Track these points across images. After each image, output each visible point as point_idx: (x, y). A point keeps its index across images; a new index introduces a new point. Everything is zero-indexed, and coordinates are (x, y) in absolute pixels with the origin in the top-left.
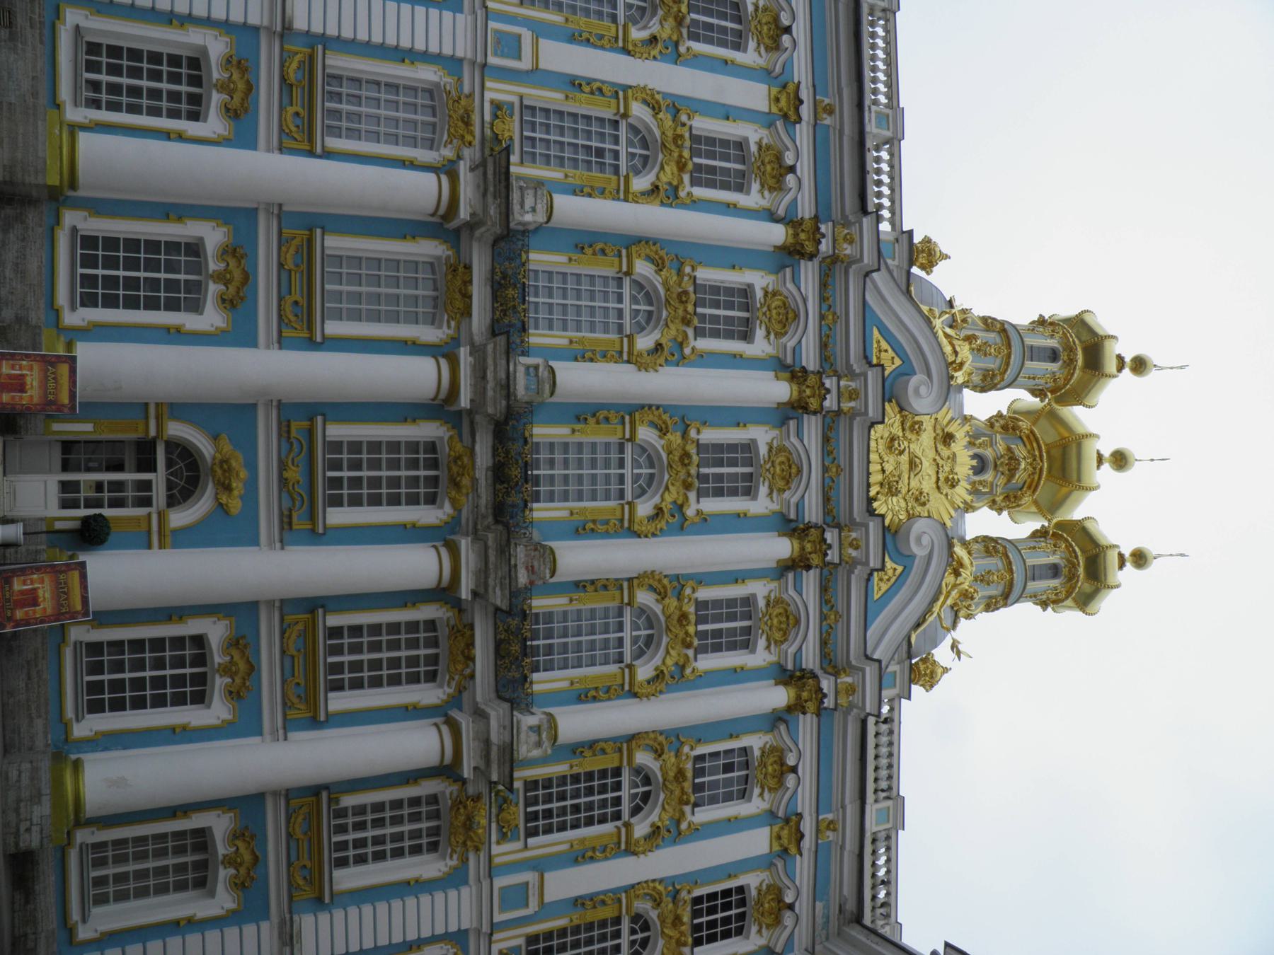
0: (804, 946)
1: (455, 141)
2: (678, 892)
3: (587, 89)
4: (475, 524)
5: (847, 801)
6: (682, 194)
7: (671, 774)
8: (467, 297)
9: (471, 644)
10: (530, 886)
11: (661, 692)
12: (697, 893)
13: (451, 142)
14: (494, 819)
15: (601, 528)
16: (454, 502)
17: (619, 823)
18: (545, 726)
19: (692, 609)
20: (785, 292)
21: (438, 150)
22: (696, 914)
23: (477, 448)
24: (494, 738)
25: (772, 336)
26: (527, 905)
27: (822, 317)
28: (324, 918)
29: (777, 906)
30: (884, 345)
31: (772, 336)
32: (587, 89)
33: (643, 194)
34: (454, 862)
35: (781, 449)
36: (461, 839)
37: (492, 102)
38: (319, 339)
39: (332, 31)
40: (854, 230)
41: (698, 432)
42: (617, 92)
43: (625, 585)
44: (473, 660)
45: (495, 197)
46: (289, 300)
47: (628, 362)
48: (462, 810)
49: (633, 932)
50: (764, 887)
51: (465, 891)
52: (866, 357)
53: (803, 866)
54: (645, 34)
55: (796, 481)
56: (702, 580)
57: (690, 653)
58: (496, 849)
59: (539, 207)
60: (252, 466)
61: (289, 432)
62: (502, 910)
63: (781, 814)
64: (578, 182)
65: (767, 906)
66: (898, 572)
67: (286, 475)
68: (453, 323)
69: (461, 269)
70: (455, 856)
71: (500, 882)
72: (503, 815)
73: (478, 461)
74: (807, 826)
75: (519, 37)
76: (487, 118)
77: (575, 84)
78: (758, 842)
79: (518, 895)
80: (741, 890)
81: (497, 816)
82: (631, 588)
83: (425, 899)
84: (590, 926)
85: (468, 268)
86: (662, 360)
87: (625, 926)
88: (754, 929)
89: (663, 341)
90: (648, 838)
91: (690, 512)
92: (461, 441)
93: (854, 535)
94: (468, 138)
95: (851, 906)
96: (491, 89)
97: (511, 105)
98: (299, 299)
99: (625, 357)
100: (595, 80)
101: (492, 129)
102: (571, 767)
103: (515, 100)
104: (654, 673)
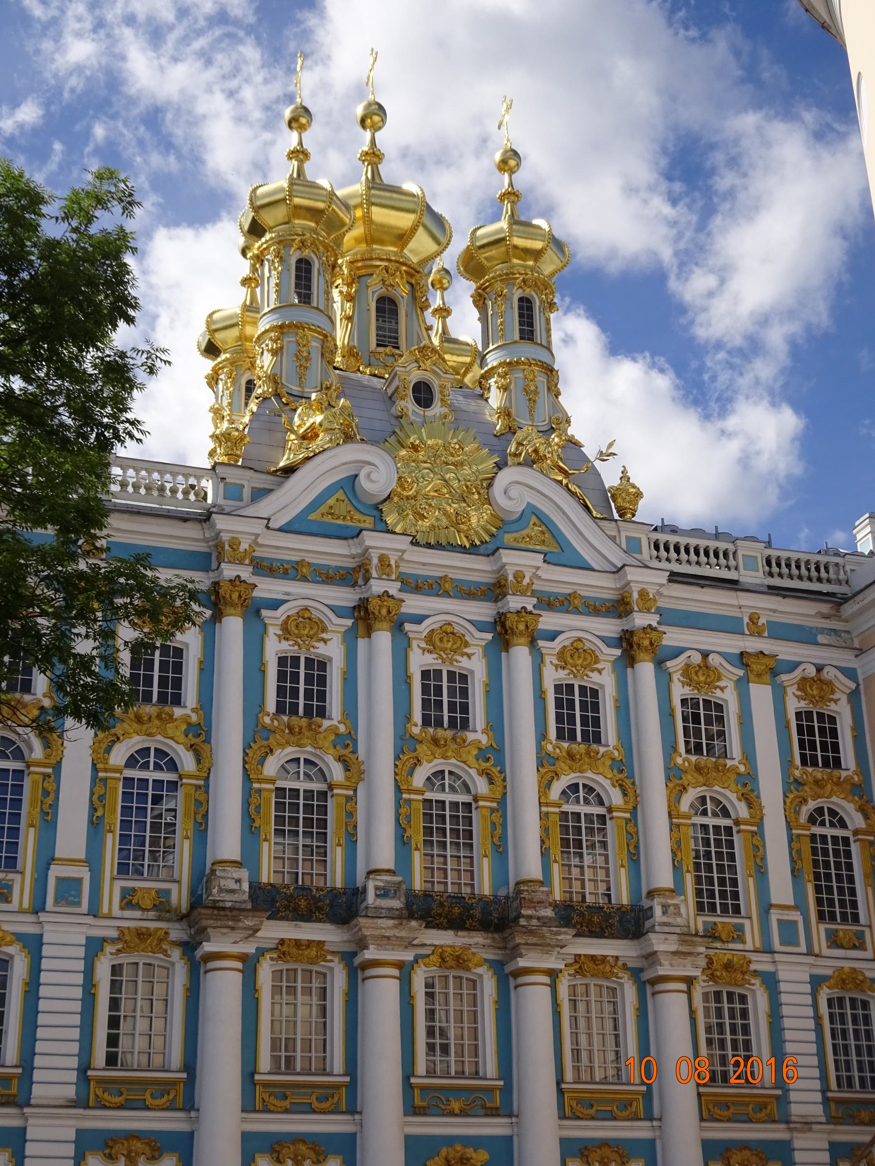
0: (853, 658)
1: (164, 947)
2: (796, 780)
3: (99, 813)
4: (499, 948)
5: (735, 603)
6: (194, 718)
7: (701, 779)
8: (309, 944)
9: (593, 958)
10: (780, 917)
11: (633, 784)
12: (798, 761)
13: (166, 951)
14: (726, 946)
15: (499, 831)
16: (479, 965)
17: (735, 829)
18: (663, 900)
19: (565, 745)
20: (284, 617)
21: (173, 964)
22: (815, 764)
23: (436, 943)
24: (673, 948)
25: (324, 636)
26: (795, 922)
27: (304, 579)
28: (793, 1096)
29: (816, 685)
30: (324, 509)
31: (324, 636)
32: (99, 813)
33: (199, 761)
34: (757, 982)
35: (430, 638)
36: (739, 976)
37: (122, 908)
38: (348, 1079)
39: (74, 1062)
40: (225, 537)
41: (416, 725)
42: (101, 780)
43: (544, 809)
44: (605, 957)
45: (239, 920)
46: (316, 1105)
47: (355, 791)
48: (718, 974)
49: (823, 824)
50: (799, 693)
51: (781, 976)
52: (346, 539)
53: (786, 651)
54: (36, 743)
55: (457, 629)
56: (542, 735)
57: (602, 750)
58: (749, 946)
59: (236, 875)
60: (450, 1140)
61: (424, 1108)
62: (798, 945)
63: (741, 673)
64: (192, 826)
65: (815, 693)
66: (538, 523)
67: (457, 1111)
68: (329, 957)
69: (285, 948)
70: (753, 981)
71: (777, 946)
72: (723, 937)
73: (449, 942)
74: (752, 645)
75: (60, 880)
76: (137, 914)
77: (96, 824)
78: (761, 695)
79: (787, 927)
80: (798, 715)
81: (723, 942)
82: (547, 805)
83: (785, 1010)
84: (815, 863)
85: (282, 942)
86: (353, 757)
87: (817, 830)
88: (833, 706)
89: (337, 754)
90: (750, 805)
91: (484, 740)
92: (428, 956)
93: (511, 578)
94: (161, 934)
95: (825, 608)
96: (110, 909)
97: (123, 889)
98: (314, 1098)
99: (351, 793)
100: (91, 801)
101: (148, 910)
102: (688, 871)
103: (119, 884)
104: (618, 789)
